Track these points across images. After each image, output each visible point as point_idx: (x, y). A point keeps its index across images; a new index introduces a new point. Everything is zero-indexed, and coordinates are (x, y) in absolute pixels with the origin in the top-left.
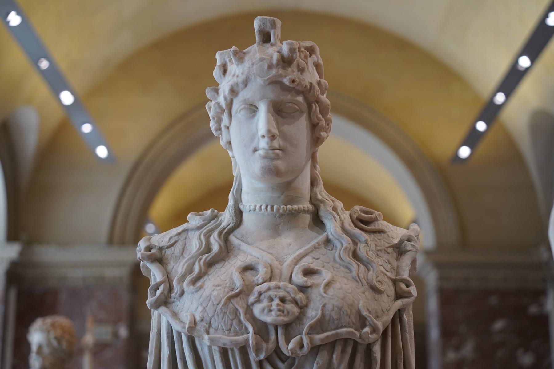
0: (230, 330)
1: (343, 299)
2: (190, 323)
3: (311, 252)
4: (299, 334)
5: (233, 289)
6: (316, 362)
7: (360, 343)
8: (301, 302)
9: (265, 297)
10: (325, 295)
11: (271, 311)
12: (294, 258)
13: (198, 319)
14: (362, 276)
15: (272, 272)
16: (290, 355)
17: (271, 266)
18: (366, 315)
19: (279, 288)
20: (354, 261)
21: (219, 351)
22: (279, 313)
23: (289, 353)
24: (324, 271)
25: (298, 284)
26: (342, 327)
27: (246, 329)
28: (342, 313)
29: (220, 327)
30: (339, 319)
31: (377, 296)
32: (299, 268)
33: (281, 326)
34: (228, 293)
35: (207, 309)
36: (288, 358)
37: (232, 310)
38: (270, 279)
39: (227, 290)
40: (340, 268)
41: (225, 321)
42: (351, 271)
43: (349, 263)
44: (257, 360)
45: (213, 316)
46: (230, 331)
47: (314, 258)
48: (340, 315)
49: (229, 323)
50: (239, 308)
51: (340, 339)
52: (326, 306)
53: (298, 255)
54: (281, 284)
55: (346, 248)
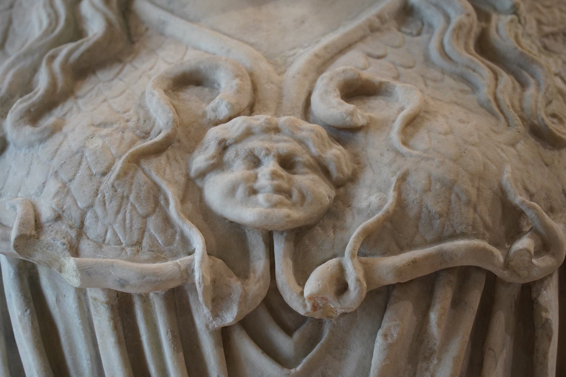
0: (139, 243)
1: (455, 160)
2: (23, 224)
3: (362, 39)
4: (335, 256)
5: (146, 135)
6: (380, 332)
7: (503, 282)
8: (339, 169)
9: (237, 155)
10: (404, 149)
11: (254, 192)
12: (317, 56)
13: (46, 213)
14: (505, 100)
15: (255, 89)
16: (308, 313)
17: (251, 74)
18: (523, 202)
19: (277, 130)
20: (483, 62)
21: (107, 303)
22: (277, 197)
23: (305, 306)
24: (399, 88)
25: (331, 122)
26: (454, 236)
27: (186, 242)
28: (453, 197)
29: (109, 235)
30: (446, 214)
31: (548, 154)
32: (331, 79)
33: (282, 233)
34: (133, 143)
35: (73, 186)
36: (301, 320)
37: (144, 188)
38: (251, 110)
39: (128, 135)
40: (442, 80)
41: (124, 220)
42: (474, 88)
43: (468, 67)
44: (216, 326)
45: (91, 206)
46: (137, 247)
47: (369, 55)
48: (450, 202)
49: (137, 224)
50: (164, 185)
51: (449, 270)
52: (410, 179)
53: (326, 48)
54: (282, 120)
55: (460, 27)
